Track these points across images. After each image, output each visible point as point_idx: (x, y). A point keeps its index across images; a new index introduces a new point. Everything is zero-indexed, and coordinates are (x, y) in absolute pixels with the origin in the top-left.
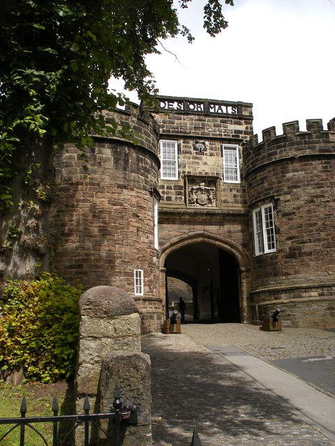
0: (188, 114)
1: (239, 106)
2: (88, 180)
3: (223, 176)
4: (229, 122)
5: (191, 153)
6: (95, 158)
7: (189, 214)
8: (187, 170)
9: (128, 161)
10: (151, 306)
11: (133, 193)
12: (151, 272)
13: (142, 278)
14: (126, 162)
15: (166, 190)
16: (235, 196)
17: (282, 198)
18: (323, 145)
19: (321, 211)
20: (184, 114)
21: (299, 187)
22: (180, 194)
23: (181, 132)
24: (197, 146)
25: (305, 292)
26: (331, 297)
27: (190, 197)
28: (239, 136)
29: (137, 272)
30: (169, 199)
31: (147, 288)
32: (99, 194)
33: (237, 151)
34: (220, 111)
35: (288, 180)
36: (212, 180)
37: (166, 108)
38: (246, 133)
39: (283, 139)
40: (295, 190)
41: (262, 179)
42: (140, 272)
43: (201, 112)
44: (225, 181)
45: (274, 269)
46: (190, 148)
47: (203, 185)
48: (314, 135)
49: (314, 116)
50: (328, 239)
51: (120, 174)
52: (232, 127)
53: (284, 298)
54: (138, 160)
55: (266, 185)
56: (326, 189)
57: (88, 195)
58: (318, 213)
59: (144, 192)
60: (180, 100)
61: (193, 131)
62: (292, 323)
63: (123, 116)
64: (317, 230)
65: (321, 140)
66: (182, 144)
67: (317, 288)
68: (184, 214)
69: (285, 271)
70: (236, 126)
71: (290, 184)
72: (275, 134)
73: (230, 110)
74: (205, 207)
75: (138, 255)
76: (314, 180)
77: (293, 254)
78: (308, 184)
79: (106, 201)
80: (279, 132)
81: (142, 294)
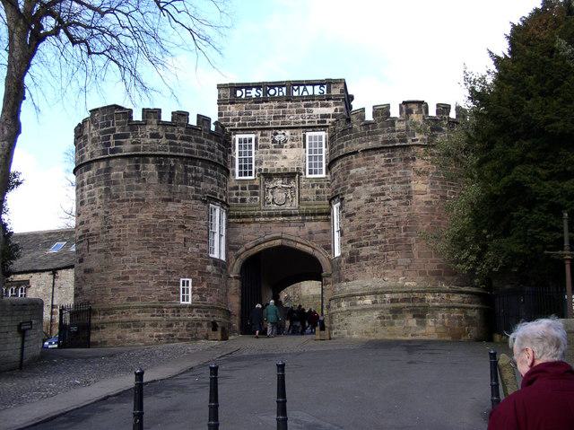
0: (266, 102)
1: (329, 83)
3: (305, 171)
5: (269, 147)
8: (263, 167)
11: (180, 205)
12: (203, 280)
14: (172, 175)
15: (240, 191)
17: (347, 197)
19: (380, 211)
22: (256, 194)
23: (259, 124)
24: (277, 138)
25: (360, 299)
28: (325, 122)
29: (184, 282)
30: (243, 200)
31: (197, 297)
34: (305, 94)
35: (351, 177)
36: (290, 176)
37: (243, 97)
38: (334, 116)
42: (188, 282)
44: (308, 176)
45: (339, 274)
46: (268, 141)
47: (279, 183)
49: (381, 101)
51: (164, 188)
53: (344, 305)
54: (186, 170)
56: (387, 186)
58: (376, 214)
59: (193, 202)
60: (258, 86)
63: (169, 128)
66: (259, 138)
70: (322, 109)
71: (353, 181)
73: (317, 90)
77: (351, 260)
81: (190, 302)
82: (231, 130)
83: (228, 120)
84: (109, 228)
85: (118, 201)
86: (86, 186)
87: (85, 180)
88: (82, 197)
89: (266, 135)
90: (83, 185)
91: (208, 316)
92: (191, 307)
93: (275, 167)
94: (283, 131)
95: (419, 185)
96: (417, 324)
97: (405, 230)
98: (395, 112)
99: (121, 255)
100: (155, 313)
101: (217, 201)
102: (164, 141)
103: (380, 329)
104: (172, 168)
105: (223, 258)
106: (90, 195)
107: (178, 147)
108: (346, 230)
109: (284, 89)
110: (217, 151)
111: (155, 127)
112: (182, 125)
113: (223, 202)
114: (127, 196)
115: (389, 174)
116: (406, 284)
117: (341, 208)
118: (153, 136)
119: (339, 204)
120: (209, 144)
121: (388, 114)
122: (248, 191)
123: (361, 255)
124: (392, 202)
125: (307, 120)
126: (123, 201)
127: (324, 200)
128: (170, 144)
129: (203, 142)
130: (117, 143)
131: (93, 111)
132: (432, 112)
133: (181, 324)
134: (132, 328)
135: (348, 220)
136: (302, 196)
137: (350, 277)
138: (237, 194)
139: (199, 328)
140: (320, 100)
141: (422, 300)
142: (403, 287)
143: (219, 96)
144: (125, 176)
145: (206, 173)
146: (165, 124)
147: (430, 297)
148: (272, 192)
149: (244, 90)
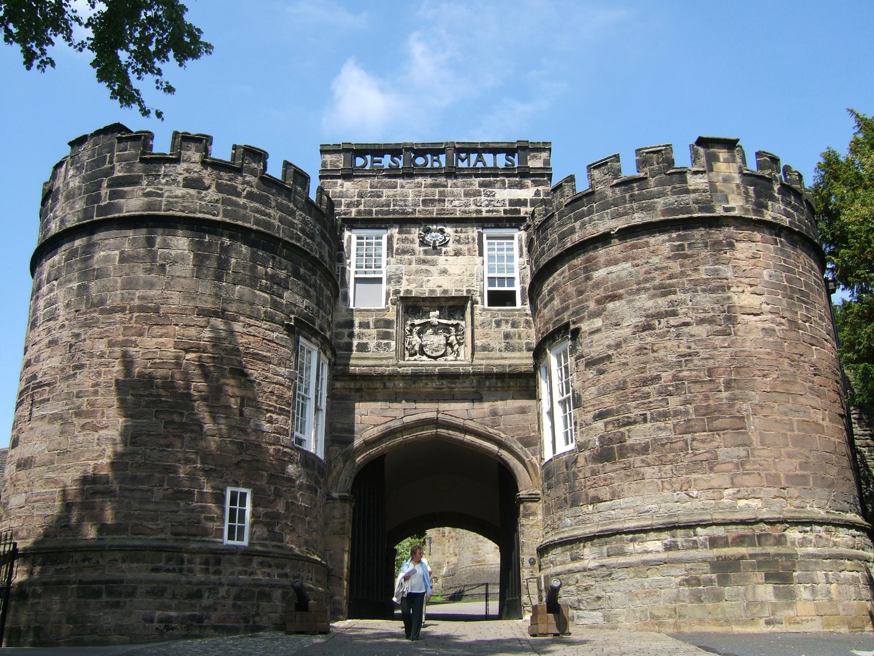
0: (410, 176)
2: (136, 302)
3: (482, 295)
4: (498, 185)
5: (413, 252)
6: (153, 259)
7: (404, 377)
8: (403, 287)
9: (227, 261)
10: (267, 570)
12: (278, 494)
13: (248, 508)
14: (223, 265)
16: (507, 336)
17: (585, 326)
18: (671, 199)
20: (402, 176)
21: (619, 297)
22: (387, 336)
23: (394, 212)
24: (428, 238)
25: (632, 540)
26: (693, 553)
28: (519, 212)
29: (234, 495)
31: (261, 531)
32: (156, 330)
33: (516, 242)
34: (480, 165)
35: (597, 285)
38: (533, 203)
39: (590, 195)
40: (610, 305)
41: (550, 292)
42: (243, 495)
43: (440, 168)
45: (572, 489)
46: (413, 242)
47: (434, 317)
48: (652, 181)
50: (687, 412)
51: (206, 287)
52: (504, 194)
53: (590, 556)
54: (254, 259)
55: (556, 302)
56: (680, 296)
57: (133, 331)
58: (662, 353)
60: (395, 151)
61: (421, 207)
62: (606, 618)
64: (660, 393)
65: (669, 188)
66: (396, 236)
67: (659, 530)
68: (392, 376)
69: (592, 493)
71: (600, 293)
72: (574, 190)
73: (501, 160)
74: (441, 361)
75: (239, 458)
76: (653, 279)
78: (638, 290)
79: (169, 342)
80: (582, 185)
81: (245, 543)
84: (77, 367)
85: (102, 312)
86: (45, 289)
87: (45, 276)
88: (35, 311)
90: (39, 288)
91: (285, 575)
92: (247, 554)
95: (744, 299)
96: (776, 596)
97: (728, 385)
98: (682, 159)
99: (96, 429)
100: (162, 564)
102: (212, 194)
103: (692, 609)
104: (225, 250)
105: (321, 455)
106: (50, 304)
107: (242, 211)
108: (588, 395)
109: (443, 158)
110: (318, 239)
111: (198, 167)
112: (253, 172)
113: (324, 337)
114: (123, 299)
115: (683, 274)
116: (742, 503)
117: (573, 349)
118: (194, 183)
121: (670, 162)
122: (373, 331)
123: (629, 442)
124: (695, 329)
125: (484, 209)
126: (113, 310)
127: (520, 350)
128: (225, 202)
130: (113, 195)
131: (76, 143)
132: (752, 165)
133: (222, 591)
134: (105, 598)
135: (591, 374)
136: (478, 343)
137: (604, 492)
139: (264, 604)
140: (508, 176)
141: (780, 540)
142: (733, 509)
143: (324, 164)
144: (123, 259)
146: (218, 165)
147: (794, 534)
149: (369, 157)
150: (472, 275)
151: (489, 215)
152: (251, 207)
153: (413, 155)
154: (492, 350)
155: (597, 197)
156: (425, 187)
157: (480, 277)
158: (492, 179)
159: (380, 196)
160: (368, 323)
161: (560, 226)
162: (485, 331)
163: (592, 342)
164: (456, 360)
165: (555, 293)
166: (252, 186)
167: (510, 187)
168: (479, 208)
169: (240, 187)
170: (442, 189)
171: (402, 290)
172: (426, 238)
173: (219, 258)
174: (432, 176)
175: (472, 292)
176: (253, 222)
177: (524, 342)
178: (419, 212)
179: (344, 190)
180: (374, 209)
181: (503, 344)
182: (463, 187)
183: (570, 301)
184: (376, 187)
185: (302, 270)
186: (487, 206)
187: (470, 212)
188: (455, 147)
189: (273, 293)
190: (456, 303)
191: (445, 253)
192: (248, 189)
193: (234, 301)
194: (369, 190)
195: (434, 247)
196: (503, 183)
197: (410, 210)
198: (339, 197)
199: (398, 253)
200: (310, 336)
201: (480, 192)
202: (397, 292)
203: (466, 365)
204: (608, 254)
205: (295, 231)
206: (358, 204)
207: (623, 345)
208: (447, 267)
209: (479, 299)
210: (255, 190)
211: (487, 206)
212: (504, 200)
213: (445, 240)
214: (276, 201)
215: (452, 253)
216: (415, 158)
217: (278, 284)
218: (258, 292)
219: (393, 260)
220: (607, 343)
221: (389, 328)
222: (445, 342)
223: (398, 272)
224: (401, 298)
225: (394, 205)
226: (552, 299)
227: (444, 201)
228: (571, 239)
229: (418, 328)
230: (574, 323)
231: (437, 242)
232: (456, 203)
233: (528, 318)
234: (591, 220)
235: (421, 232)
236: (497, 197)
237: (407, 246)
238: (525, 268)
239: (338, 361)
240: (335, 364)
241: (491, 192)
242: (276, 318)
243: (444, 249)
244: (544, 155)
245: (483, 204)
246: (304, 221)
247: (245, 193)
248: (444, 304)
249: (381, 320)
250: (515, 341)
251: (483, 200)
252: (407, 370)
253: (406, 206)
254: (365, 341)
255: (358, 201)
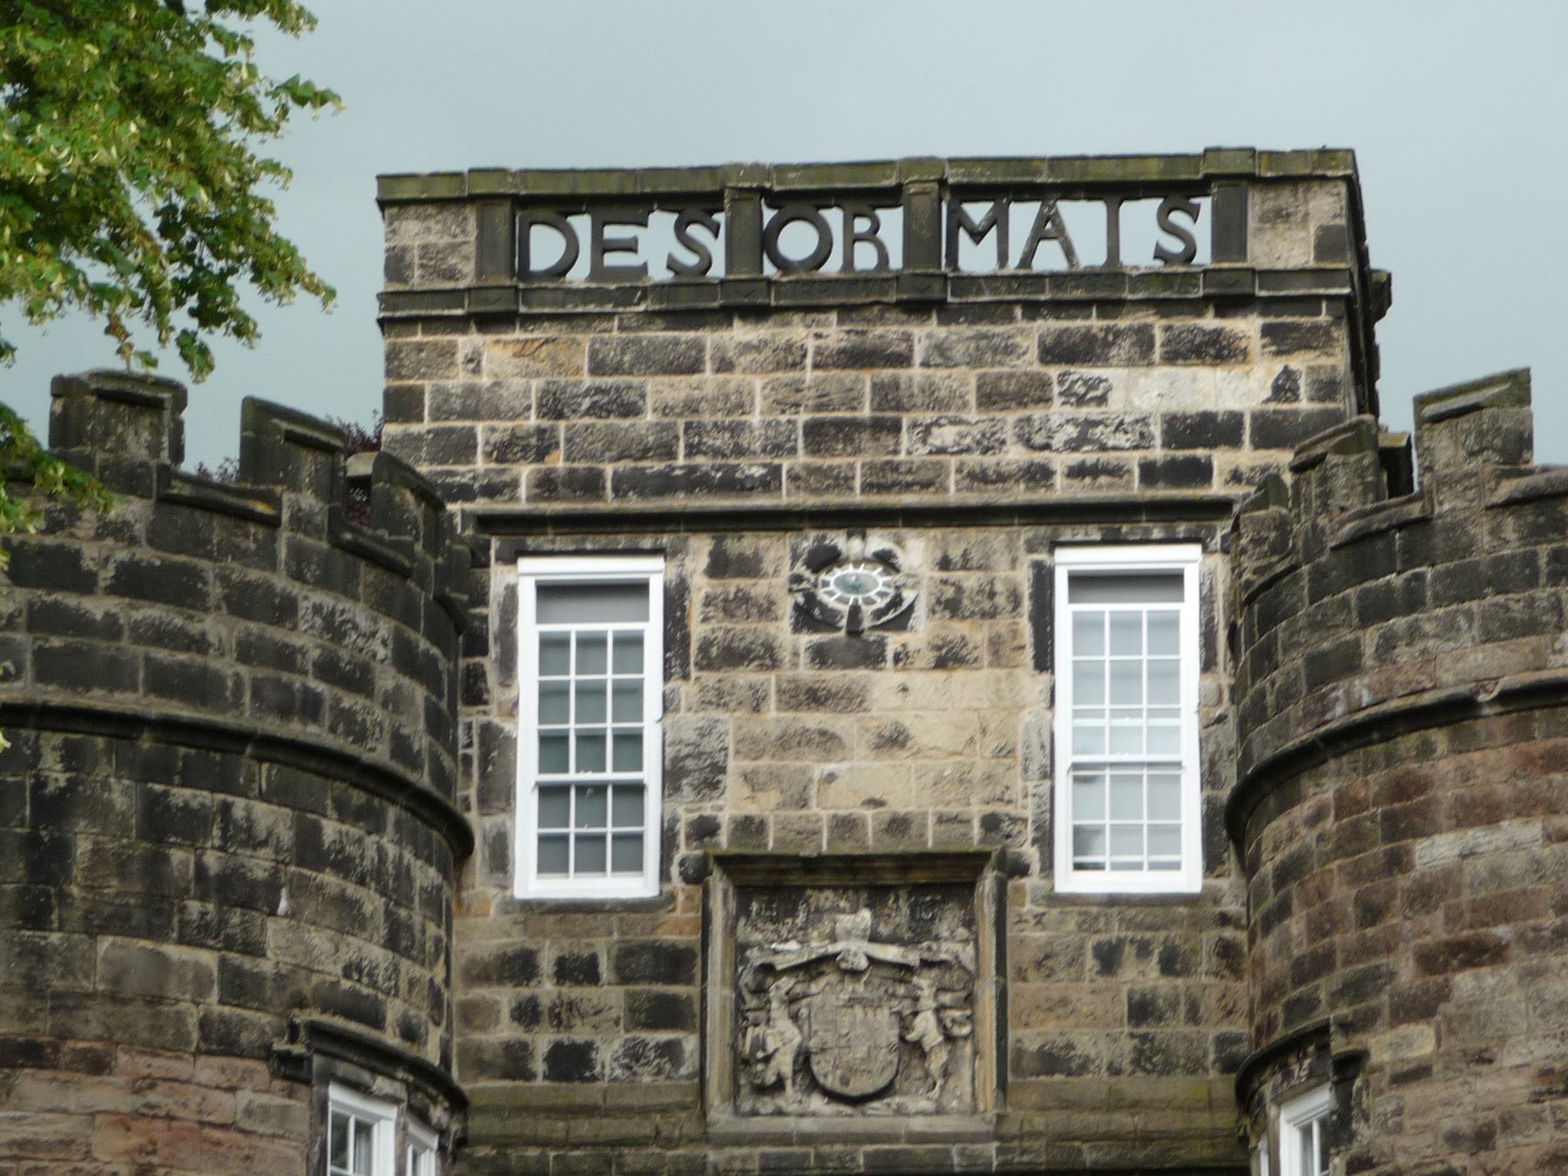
0: (757, 313)
3: (1045, 839)
5: (768, 656)
8: (729, 806)
9: (61, 850)
11: (107, 1094)
15: (547, 990)
16: (1142, 1010)
20: (725, 315)
21: (1492, 954)
22: (668, 1013)
23: (694, 481)
24: (832, 591)
27: (739, 1031)
28: (1202, 472)
33: (1188, 611)
34: (1049, 258)
35: (1426, 895)
37: (579, 275)
38: (1269, 432)
40: (1464, 982)
41: (1285, 875)
43: (878, 280)
44: (1068, 881)
46: (767, 610)
55: (1296, 925)
59: (208, 1070)
61: (802, 458)
66: (701, 586)
70: (1183, 373)
71: (1435, 928)
74: (878, 1117)
82: (487, 523)
83: (463, 447)
89: (750, 567)
93: (821, 812)
94: (878, 541)
101: (383, 1059)
109: (892, 221)
110: (387, 679)
112: (129, 480)
113: (418, 1068)
117: (1336, 1132)
119: (1322, 1100)
120: (334, 629)
122: (610, 995)
125: (1060, 462)
127: (1195, 1066)
128: (41, 619)
129: (285, 611)
138: (527, 1014)
140: (1164, 307)
143: (396, 265)
145: (308, 849)
148: (792, 999)
149: (582, 224)
150: (1005, 752)
151: (1081, 491)
152: (135, 626)
153: (769, 215)
154: (1083, 1068)
155: (1439, 541)
156: (816, 366)
157: (1039, 759)
158: (1095, 323)
159: (630, 410)
160: (593, 961)
161: (1315, 625)
162: (1056, 989)
163: (1399, 1112)
164: (939, 1111)
165: (1293, 887)
166: (133, 541)
167: (1172, 357)
168: (1039, 457)
169: (91, 553)
170: (886, 374)
171: (724, 818)
172: (821, 595)
173: (32, 842)
174: (845, 311)
175: (1006, 827)
176: (146, 680)
177: (1212, 1032)
178: (794, 478)
179: (485, 380)
180: (609, 469)
181: (1128, 1046)
182: (975, 361)
183: (1337, 938)
184: (617, 370)
185: (331, 829)
186: (1074, 445)
187: (1002, 478)
188: (942, 182)
189: (229, 944)
190: (942, 876)
191: (897, 659)
192: (122, 555)
193: (92, 996)
194: (588, 381)
195: (854, 631)
196: (1144, 340)
197: (757, 472)
198: (463, 415)
199: (707, 664)
200: (366, 1076)
201: (1045, 384)
202: (704, 829)
203: (975, 1138)
204: (1466, 776)
205: (297, 682)
206: (543, 446)
207: (1500, 1141)
208: (908, 721)
209: (1032, 854)
210: (146, 554)
211: (1074, 445)
212: (1143, 421)
213: (896, 601)
214: (224, 579)
215: (929, 657)
216: (778, 225)
217: (247, 904)
218: (174, 952)
219: (687, 691)
220: (1447, 1125)
221: (673, 979)
222: (892, 1035)
223: (710, 744)
224: (725, 862)
225: (692, 450)
226: (1283, 910)
227: (895, 428)
228: (1348, 693)
229: (786, 983)
230: (1347, 1027)
231: (867, 611)
232: (946, 435)
233: (1228, 933)
234: (1414, 634)
235: (800, 569)
236: (1116, 404)
237: (746, 629)
238: (1221, 719)
239: (477, 1125)
240: (462, 1142)
241: (1091, 384)
242: (245, 1038)
243: (893, 641)
244: (1325, 206)
245: (1057, 441)
246: (334, 629)
247: (110, 572)
248: (890, 879)
249: (644, 947)
250: (1173, 1030)
251: (1055, 421)
252: (744, 1159)
253: (739, 451)
254: (580, 1034)
255: (540, 432)
